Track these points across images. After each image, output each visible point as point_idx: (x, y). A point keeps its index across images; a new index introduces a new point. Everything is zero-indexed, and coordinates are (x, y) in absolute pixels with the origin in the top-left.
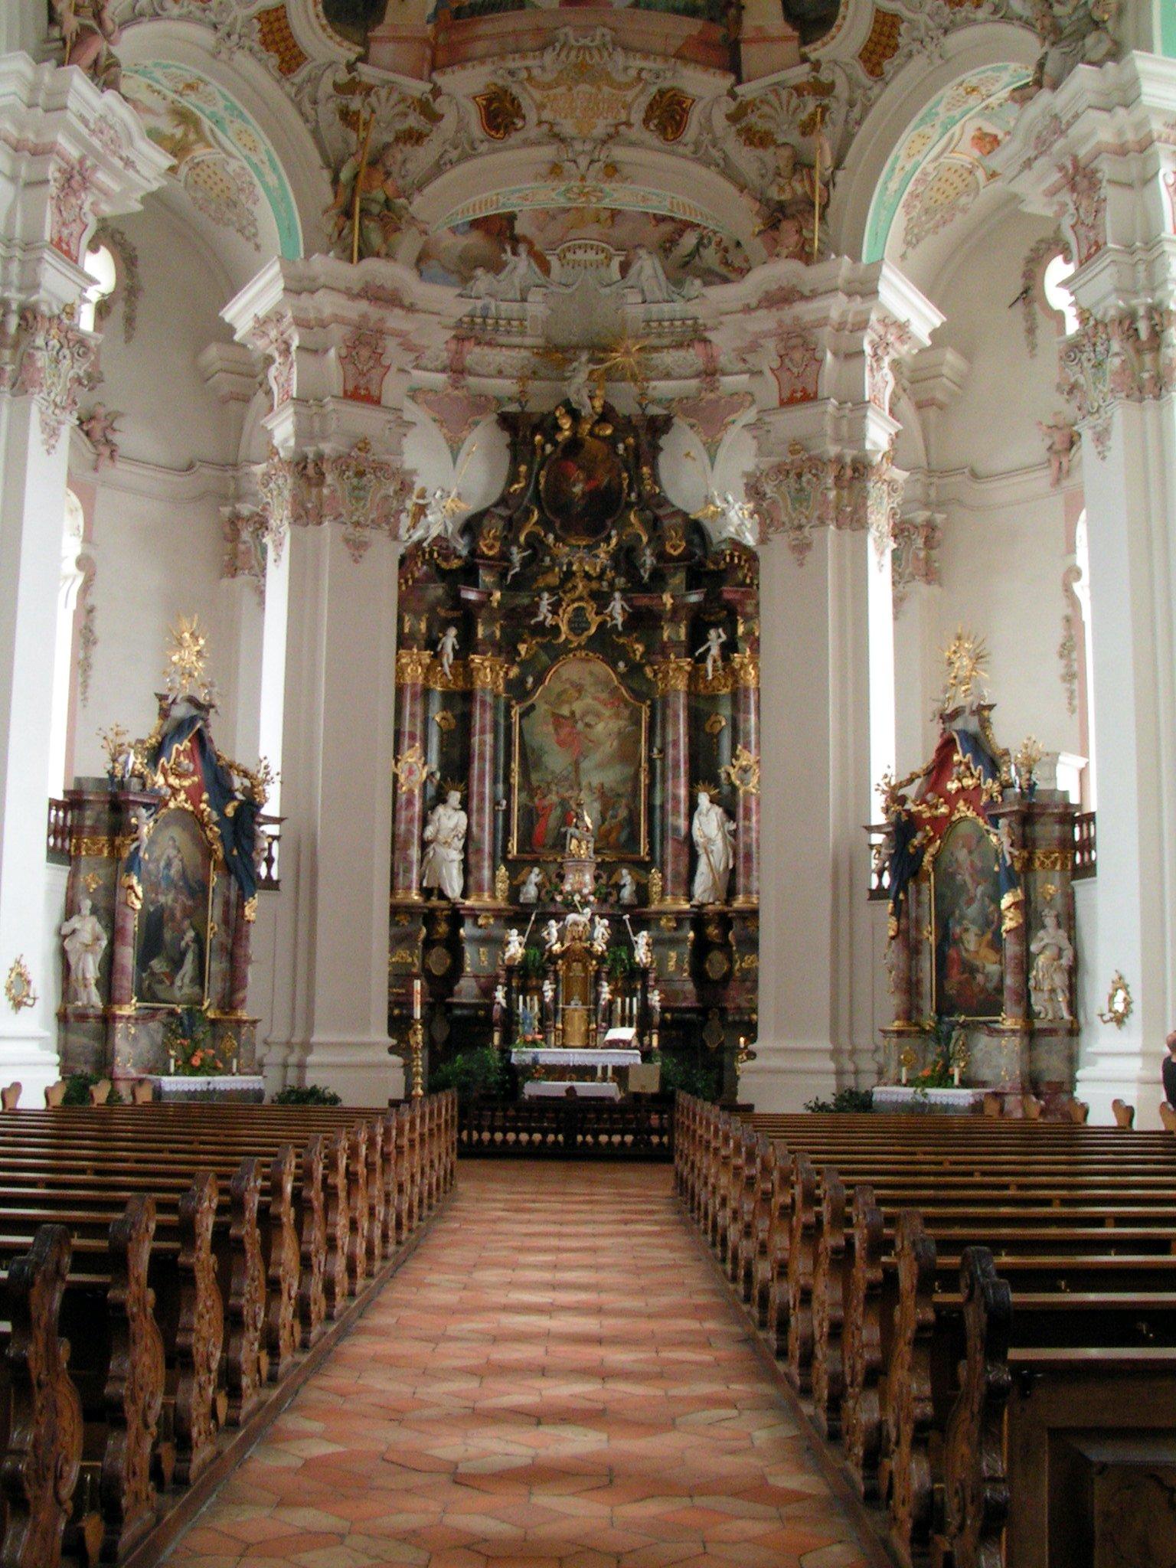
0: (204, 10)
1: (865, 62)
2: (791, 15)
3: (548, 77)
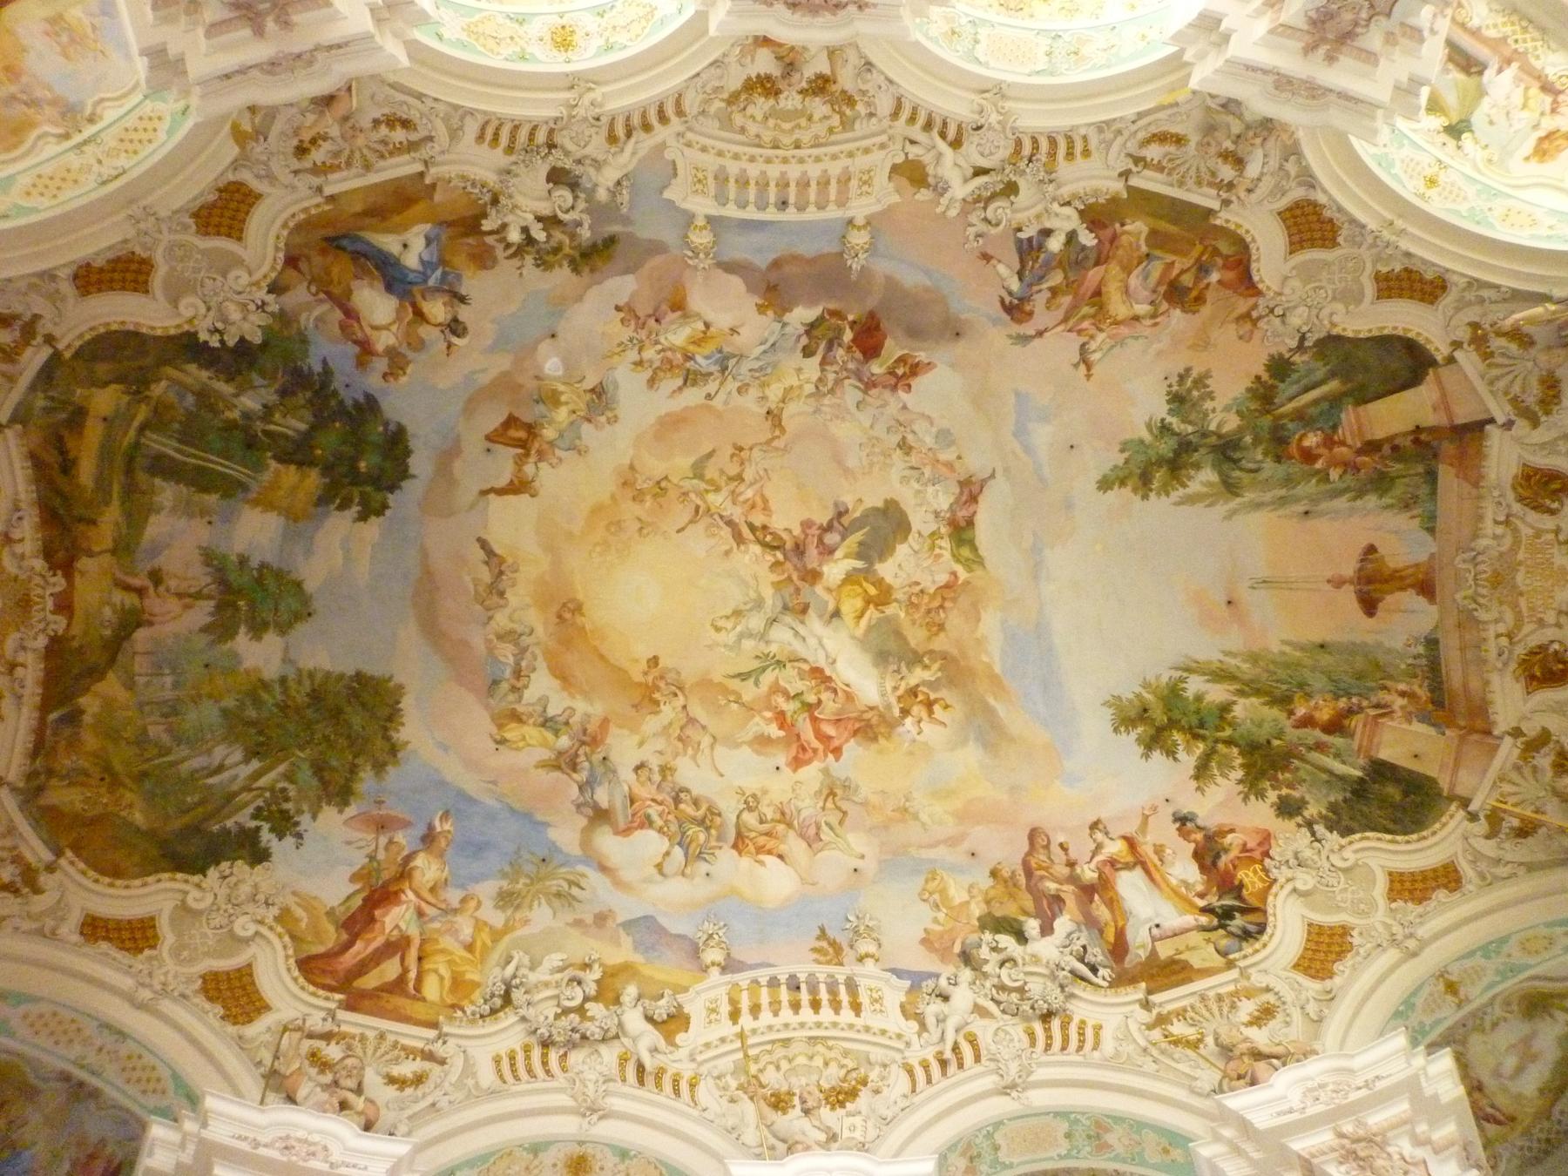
0: (1358, 953)
1: (1436, 298)
2: (1413, 379)
3: (1509, 616)
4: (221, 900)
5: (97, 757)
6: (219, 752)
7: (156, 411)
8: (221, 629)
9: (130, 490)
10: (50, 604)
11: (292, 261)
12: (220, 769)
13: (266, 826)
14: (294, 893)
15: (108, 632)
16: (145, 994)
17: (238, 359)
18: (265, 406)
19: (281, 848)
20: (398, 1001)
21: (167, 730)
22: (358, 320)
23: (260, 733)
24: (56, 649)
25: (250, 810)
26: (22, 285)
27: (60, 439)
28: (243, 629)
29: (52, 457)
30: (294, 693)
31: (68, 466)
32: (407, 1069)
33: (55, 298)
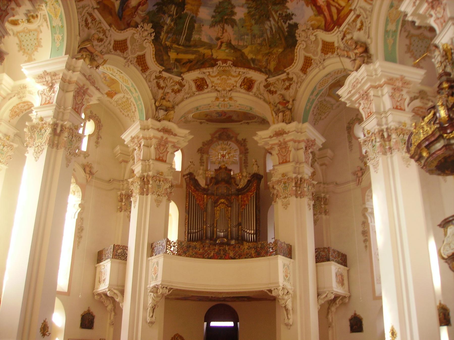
4: (305, 39)
5: (264, 56)
6: (267, 27)
7: (174, 43)
8: (233, 23)
9: (195, 46)
10: (224, 65)
11: (128, 25)
12: (271, 27)
13: (288, 21)
14: (308, 21)
15: (232, 51)
16: (321, 67)
17: (157, 27)
18: (169, 17)
19: (295, 20)
20: (343, 13)
21: (259, 39)
22: (141, 2)
23: (263, 16)
24: (235, 64)
25: (283, 24)
26: (149, 83)
27: (184, 64)
28: (233, 17)
29: (189, 65)
30: (252, 6)
31: (190, 61)
32: (359, 25)
33: (150, 75)
